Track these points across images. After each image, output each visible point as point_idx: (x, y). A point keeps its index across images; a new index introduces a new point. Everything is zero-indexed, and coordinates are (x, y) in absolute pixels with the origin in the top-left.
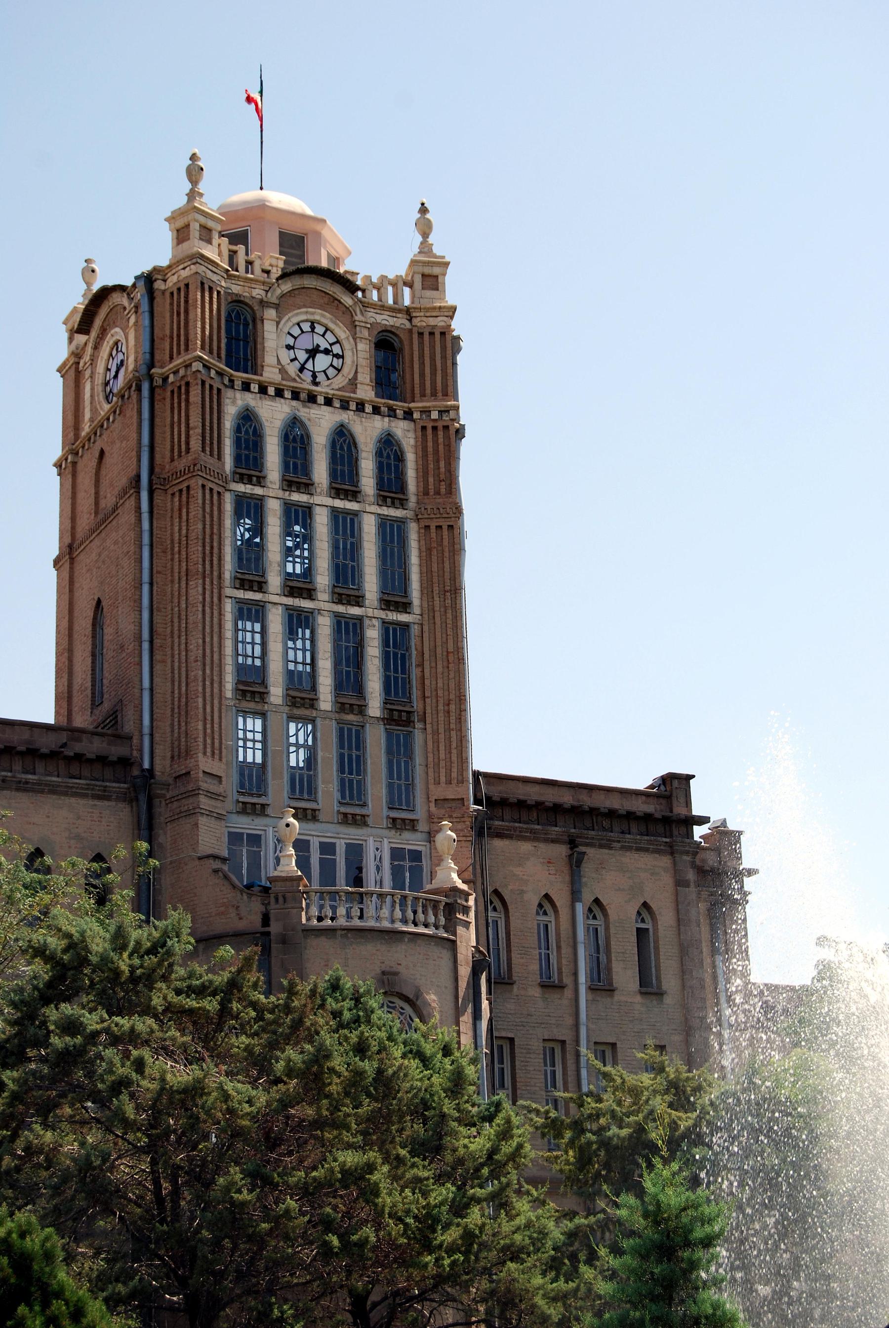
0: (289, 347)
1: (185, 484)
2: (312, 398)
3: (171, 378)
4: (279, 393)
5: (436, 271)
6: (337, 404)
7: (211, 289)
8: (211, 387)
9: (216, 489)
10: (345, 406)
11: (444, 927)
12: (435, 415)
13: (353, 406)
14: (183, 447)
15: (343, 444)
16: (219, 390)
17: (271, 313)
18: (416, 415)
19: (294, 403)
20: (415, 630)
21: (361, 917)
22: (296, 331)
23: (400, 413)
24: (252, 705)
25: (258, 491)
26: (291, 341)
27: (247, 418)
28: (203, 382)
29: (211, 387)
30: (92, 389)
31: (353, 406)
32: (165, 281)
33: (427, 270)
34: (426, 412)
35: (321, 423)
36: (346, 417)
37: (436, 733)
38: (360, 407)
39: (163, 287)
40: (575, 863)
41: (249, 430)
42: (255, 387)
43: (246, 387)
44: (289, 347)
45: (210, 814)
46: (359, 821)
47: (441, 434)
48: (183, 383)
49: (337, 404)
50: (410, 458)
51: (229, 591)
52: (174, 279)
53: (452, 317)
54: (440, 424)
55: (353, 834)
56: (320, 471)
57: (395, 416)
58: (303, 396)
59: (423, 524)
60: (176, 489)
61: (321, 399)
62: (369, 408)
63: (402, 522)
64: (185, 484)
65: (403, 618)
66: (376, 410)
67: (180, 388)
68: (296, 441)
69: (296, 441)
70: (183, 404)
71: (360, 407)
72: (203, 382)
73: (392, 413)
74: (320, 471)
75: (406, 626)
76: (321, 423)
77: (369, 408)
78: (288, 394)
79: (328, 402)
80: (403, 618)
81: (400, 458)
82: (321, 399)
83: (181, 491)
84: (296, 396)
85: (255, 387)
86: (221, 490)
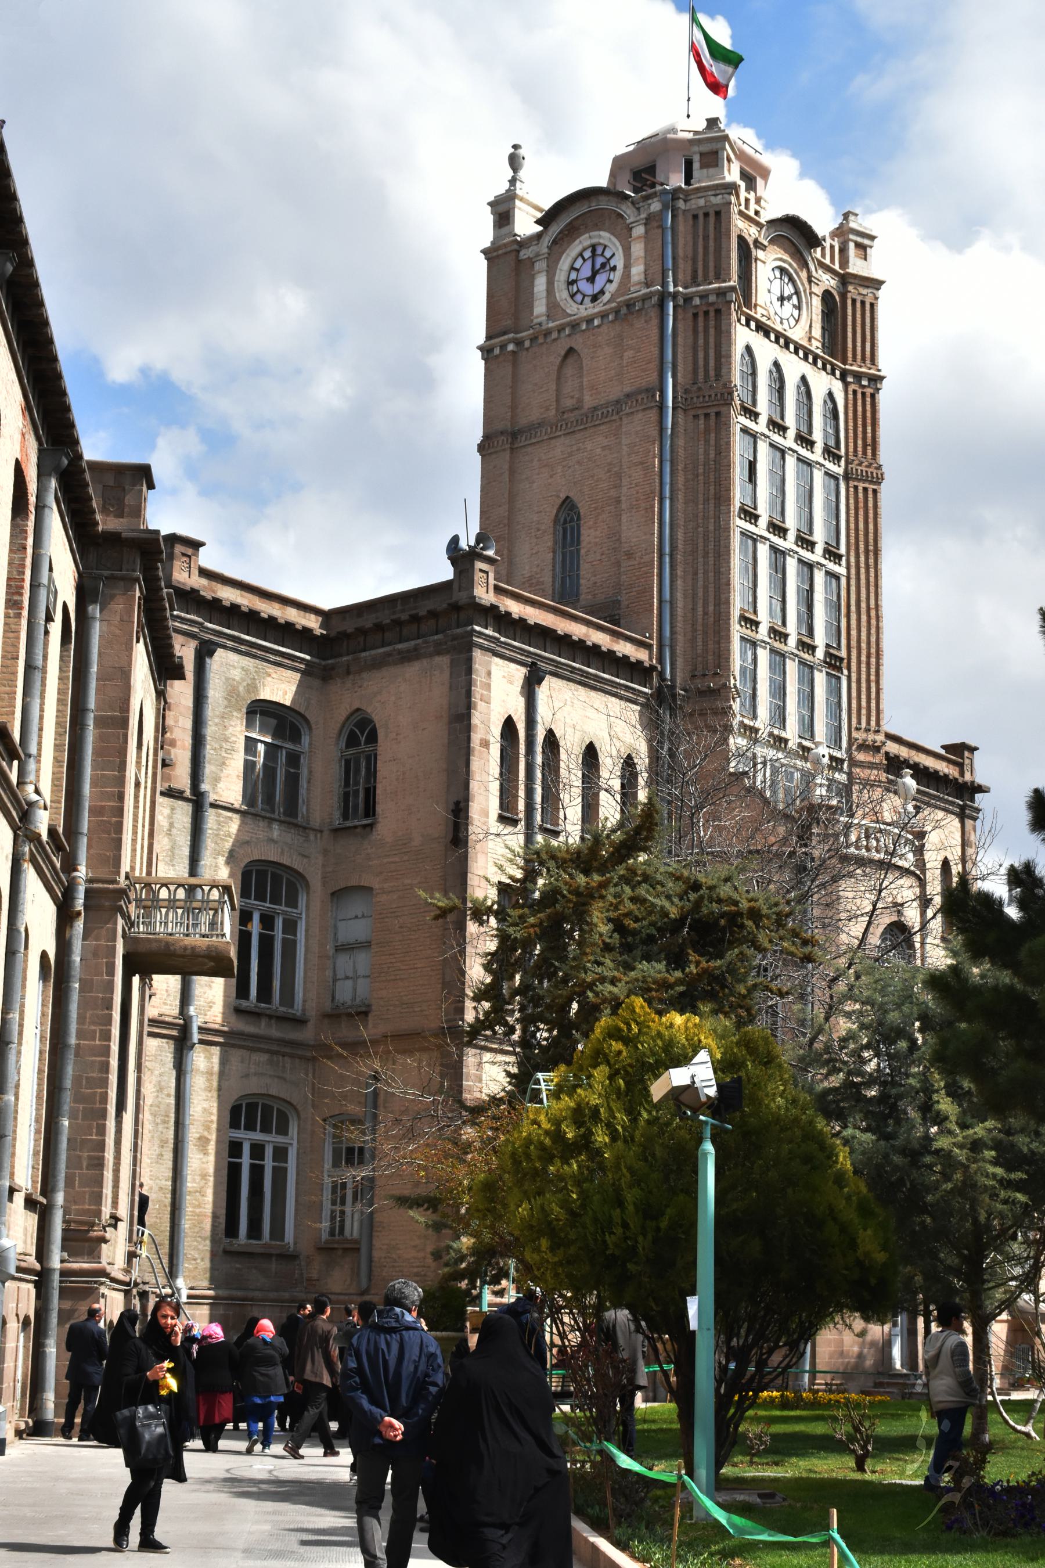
1: (715, 410)
3: (697, 301)
5: (866, 242)
14: (712, 373)
17: (760, 254)
30: (550, 283)
32: (685, 201)
33: (859, 239)
39: (683, 207)
48: (712, 309)
52: (702, 202)
53: (878, 289)
60: (700, 412)
64: (715, 410)
67: (706, 313)
70: (712, 331)
83: (707, 415)
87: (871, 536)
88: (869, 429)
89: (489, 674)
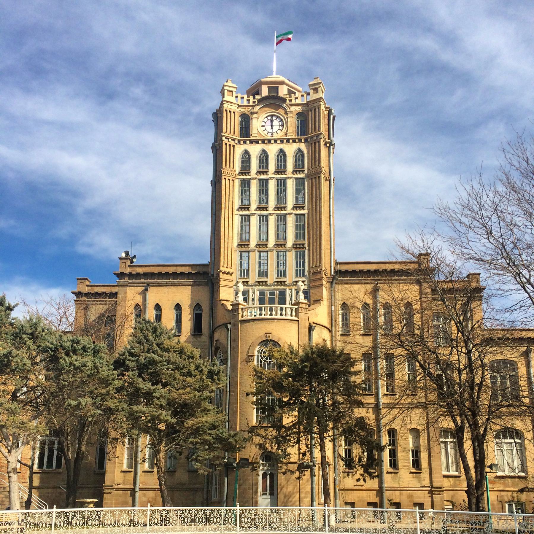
0: (263, 126)
2: (269, 141)
4: (257, 142)
6: (279, 142)
7: (230, 112)
8: (230, 145)
9: (231, 179)
10: (282, 141)
11: (295, 316)
12: (315, 138)
13: (285, 141)
15: (282, 156)
16: (234, 146)
17: (254, 116)
18: (309, 140)
19: (263, 145)
20: (306, 216)
21: (286, 315)
22: (266, 120)
23: (303, 141)
24: (244, 249)
25: (248, 177)
26: (264, 124)
27: (246, 152)
28: (226, 144)
29: (230, 145)
31: (285, 141)
34: (311, 138)
35: (273, 150)
36: (282, 146)
37: (313, 250)
38: (288, 141)
40: (376, 290)
41: (246, 157)
42: (248, 142)
43: (245, 142)
44: (263, 126)
45: (226, 286)
46: (283, 283)
47: (317, 144)
49: (279, 142)
50: (306, 155)
51: (236, 212)
54: (317, 141)
55: (282, 287)
56: (272, 166)
57: (301, 142)
58: (266, 141)
59: (310, 178)
61: (272, 142)
62: (291, 141)
63: (303, 179)
65: (302, 212)
66: (294, 141)
68: (264, 157)
69: (264, 157)
71: (288, 141)
72: (226, 144)
73: (300, 141)
74: (272, 166)
75: (303, 215)
76: (273, 150)
77: (291, 141)
78: (260, 142)
79: (276, 142)
80: (302, 212)
81: (303, 156)
82: (272, 142)
84: (263, 142)
85: (248, 142)
86: (233, 179)
87: (318, 194)
88: (317, 155)
89: (126, 293)
